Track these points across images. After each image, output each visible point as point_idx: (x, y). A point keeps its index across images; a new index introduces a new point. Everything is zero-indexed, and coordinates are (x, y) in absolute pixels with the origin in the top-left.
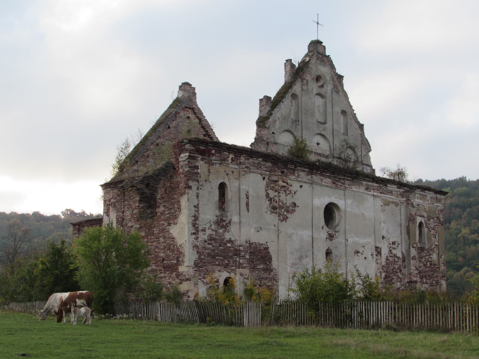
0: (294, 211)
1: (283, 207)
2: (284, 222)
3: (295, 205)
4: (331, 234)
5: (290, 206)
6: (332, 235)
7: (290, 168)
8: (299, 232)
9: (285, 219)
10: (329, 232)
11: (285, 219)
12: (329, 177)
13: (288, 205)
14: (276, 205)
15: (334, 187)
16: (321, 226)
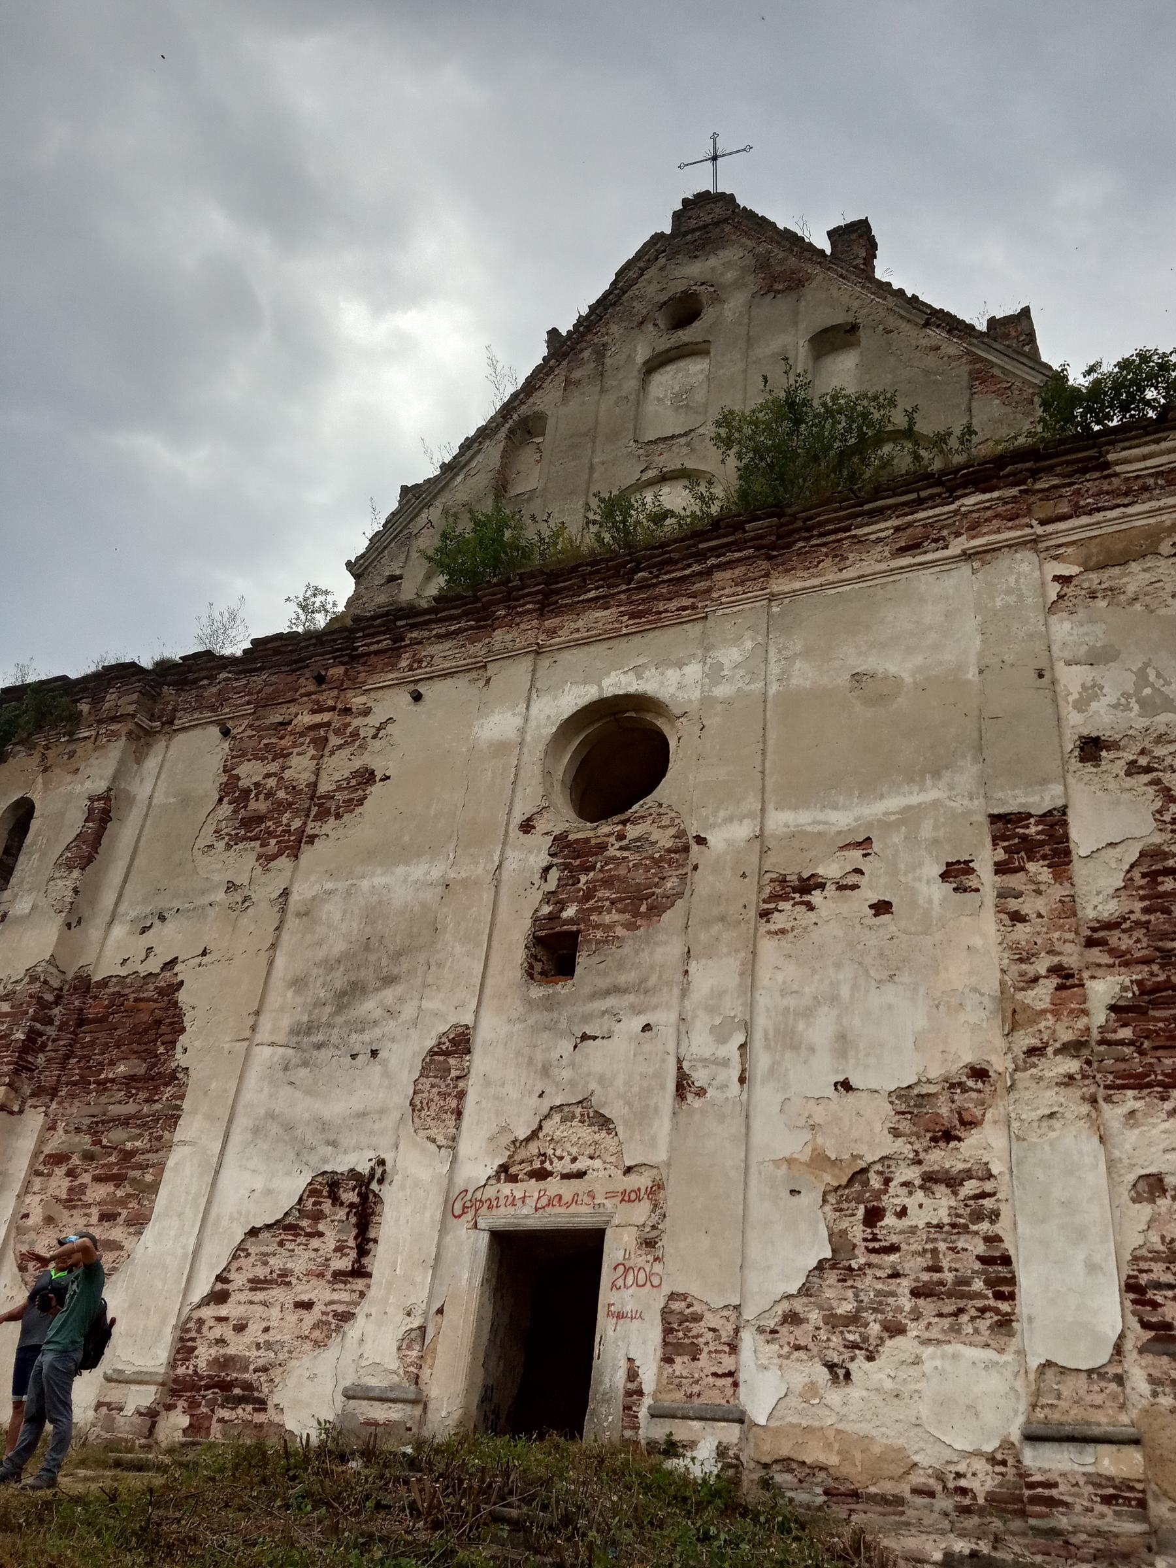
0: (361, 802)
1: (290, 804)
2: (283, 862)
3: (367, 777)
4: (587, 840)
5: (339, 788)
6: (593, 842)
7: (377, 653)
8: (365, 884)
9: (287, 848)
10: (571, 837)
11: (294, 845)
12: (603, 602)
13: (324, 787)
14: (259, 806)
15: (624, 631)
16: (518, 818)
